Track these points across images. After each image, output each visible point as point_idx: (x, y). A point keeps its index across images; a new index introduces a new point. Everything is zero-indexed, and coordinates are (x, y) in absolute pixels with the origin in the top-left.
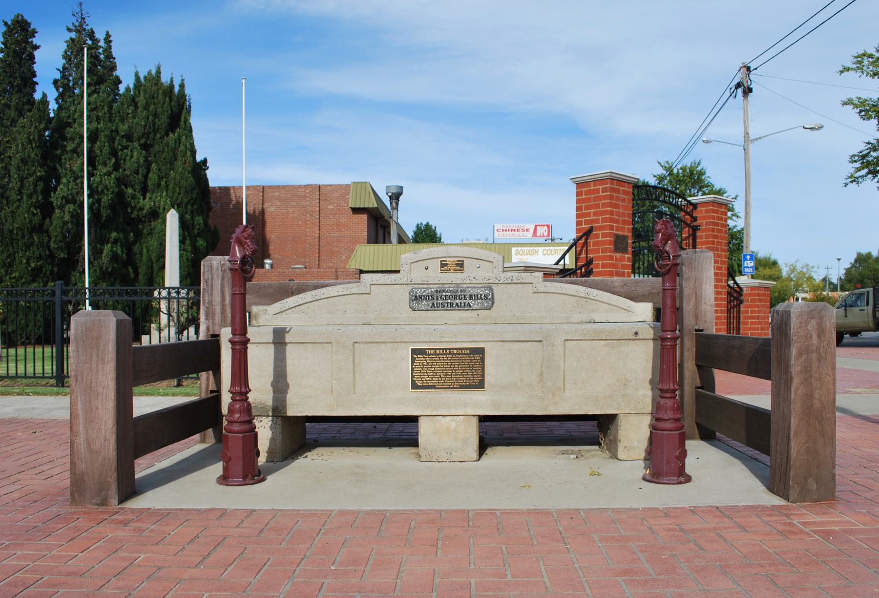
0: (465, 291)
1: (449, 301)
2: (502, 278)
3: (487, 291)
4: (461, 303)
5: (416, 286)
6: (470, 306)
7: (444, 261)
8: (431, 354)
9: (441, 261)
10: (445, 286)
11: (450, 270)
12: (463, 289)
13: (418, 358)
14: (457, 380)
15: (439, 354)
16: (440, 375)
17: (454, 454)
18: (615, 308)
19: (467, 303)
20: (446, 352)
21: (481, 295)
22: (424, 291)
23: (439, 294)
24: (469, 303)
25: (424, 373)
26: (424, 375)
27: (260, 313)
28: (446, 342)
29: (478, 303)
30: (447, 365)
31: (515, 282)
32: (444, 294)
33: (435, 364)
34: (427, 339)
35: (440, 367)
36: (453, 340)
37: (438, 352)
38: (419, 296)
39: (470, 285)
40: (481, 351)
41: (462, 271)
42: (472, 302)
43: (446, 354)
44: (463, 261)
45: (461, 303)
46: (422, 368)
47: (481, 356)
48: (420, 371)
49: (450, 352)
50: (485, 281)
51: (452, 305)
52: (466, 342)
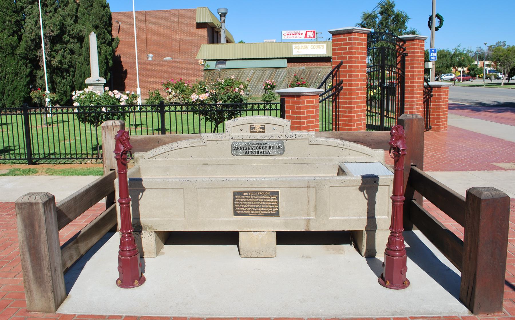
0: (266, 144)
1: (256, 150)
2: (289, 136)
3: (280, 144)
4: (264, 151)
5: (235, 141)
6: (269, 153)
7: (252, 126)
8: (245, 195)
9: (251, 126)
10: (254, 141)
11: (256, 131)
12: (264, 143)
13: (237, 197)
14: (262, 210)
15: (250, 195)
16: (252, 208)
17: (261, 253)
18: (360, 153)
19: (267, 152)
20: (255, 193)
21: (276, 147)
22: (240, 144)
23: (250, 146)
24: (268, 151)
25: (241, 206)
26: (242, 208)
27: (139, 158)
28: (254, 188)
29: (275, 151)
30: (256, 201)
31: (297, 138)
32: (253, 146)
33: (248, 201)
34: (243, 186)
35: (251, 203)
36: (259, 186)
37: (250, 194)
38: (238, 147)
39: (269, 140)
40: (277, 193)
41: (264, 132)
42: (270, 151)
43: (255, 195)
44: (264, 126)
45: (264, 151)
46: (240, 203)
47: (277, 196)
48: (239, 205)
49: (257, 194)
50: (278, 138)
51: (258, 153)
52: (267, 188)
